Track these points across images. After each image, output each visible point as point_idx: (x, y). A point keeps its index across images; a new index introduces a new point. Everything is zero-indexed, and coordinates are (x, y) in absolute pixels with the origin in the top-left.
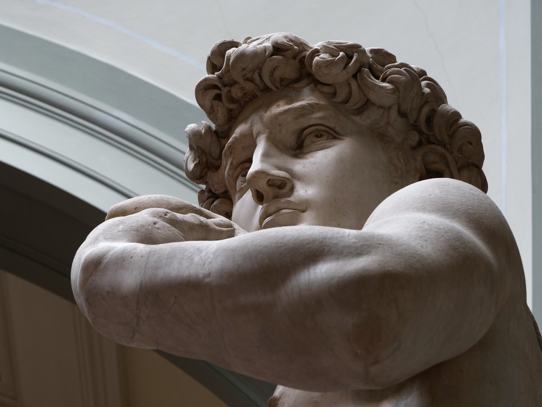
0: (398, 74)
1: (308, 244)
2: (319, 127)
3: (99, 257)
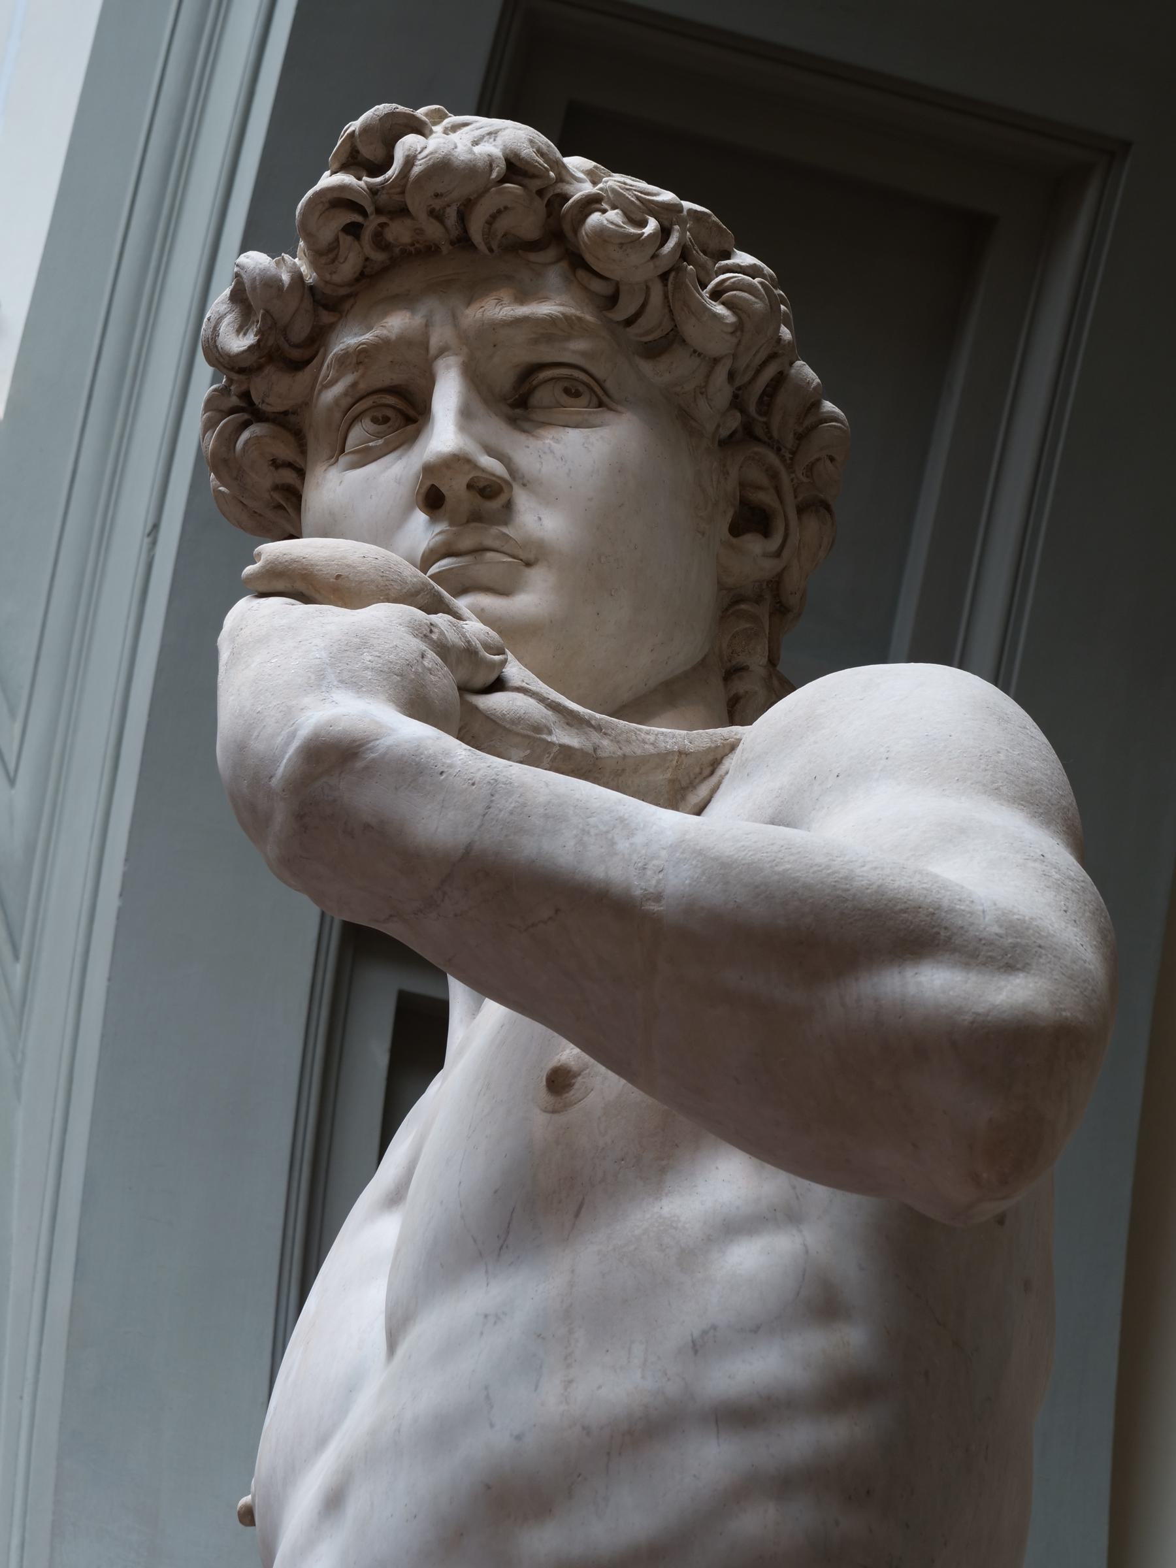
0: (750, 293)
1: (904, 911)
3: (354, 741)
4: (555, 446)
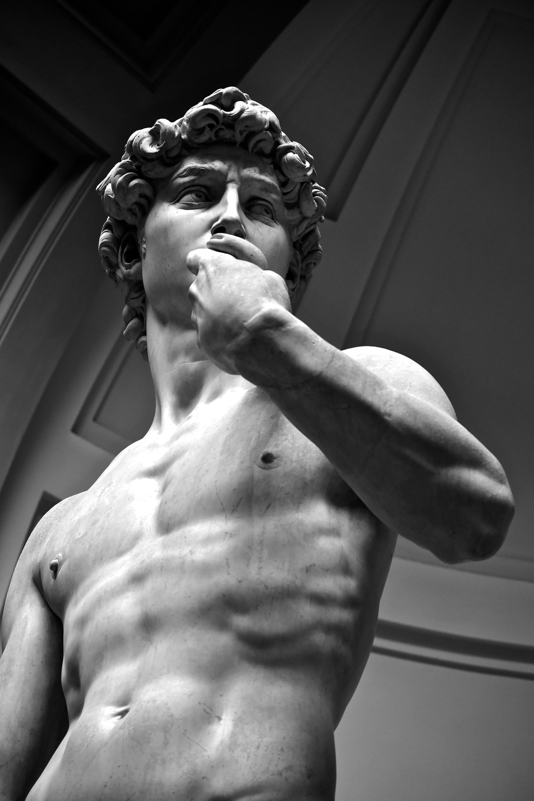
1: (474, 450)
2: (270, 206)
3: (283, 320)
4: (259, 228)
